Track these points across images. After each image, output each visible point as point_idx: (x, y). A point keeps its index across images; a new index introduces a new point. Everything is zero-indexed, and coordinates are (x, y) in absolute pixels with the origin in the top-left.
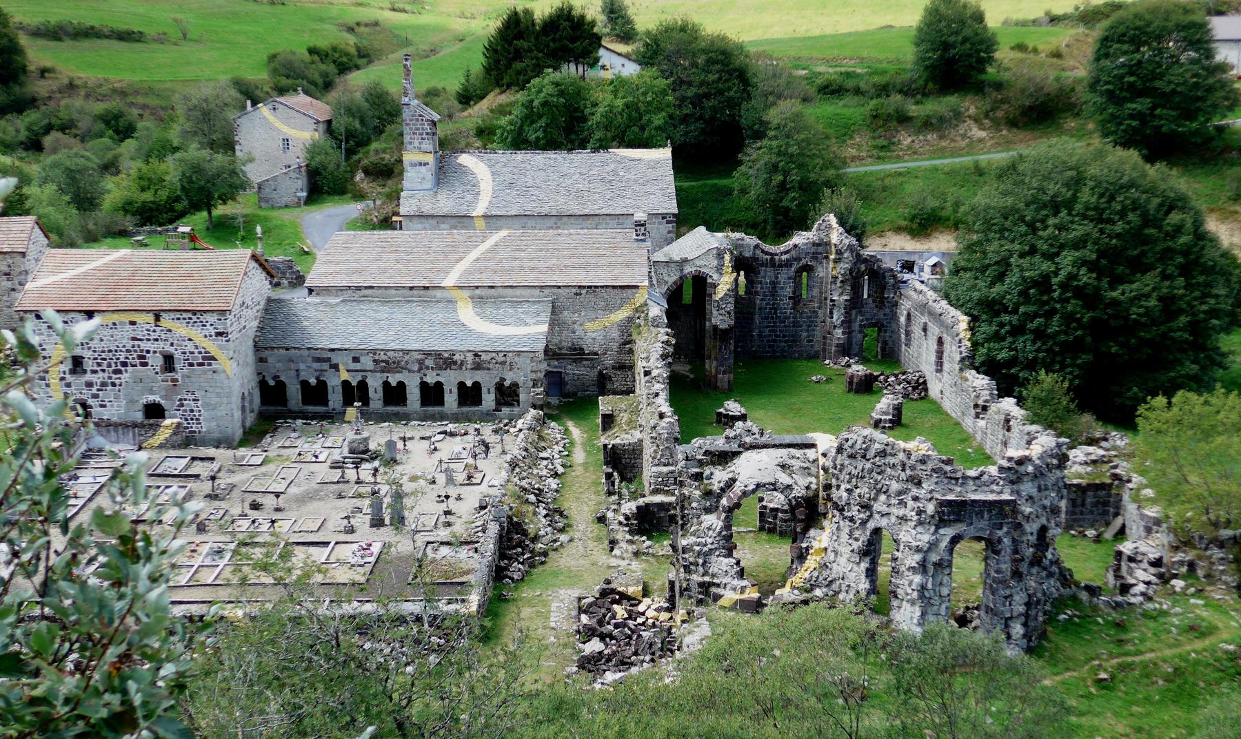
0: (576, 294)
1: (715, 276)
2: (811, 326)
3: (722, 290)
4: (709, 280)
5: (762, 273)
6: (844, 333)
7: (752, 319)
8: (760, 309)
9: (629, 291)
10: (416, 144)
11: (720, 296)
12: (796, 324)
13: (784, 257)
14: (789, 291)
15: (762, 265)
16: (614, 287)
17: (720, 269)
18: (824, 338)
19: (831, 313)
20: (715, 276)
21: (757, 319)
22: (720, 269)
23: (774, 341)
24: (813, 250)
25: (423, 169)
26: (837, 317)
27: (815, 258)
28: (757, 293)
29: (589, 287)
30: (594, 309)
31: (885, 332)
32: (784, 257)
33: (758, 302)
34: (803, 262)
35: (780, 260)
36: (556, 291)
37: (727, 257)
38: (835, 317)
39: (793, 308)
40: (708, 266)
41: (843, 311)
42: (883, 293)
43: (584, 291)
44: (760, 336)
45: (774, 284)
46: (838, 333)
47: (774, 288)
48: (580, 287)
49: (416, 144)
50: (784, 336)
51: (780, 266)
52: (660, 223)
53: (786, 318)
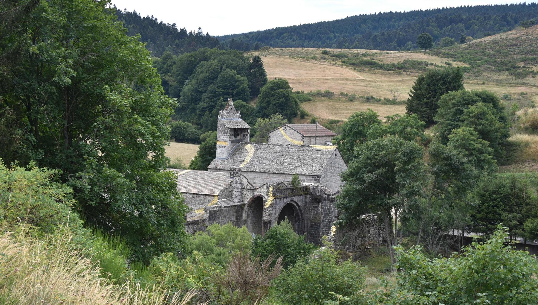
0: (193, 197)
1: (266, 197)
3: (267, 205)
4: (264, 199)
7: (319, 226)
9: (211, 197)
10: (222, 138)
11: (267, 206)
13: (333, 197)
15: (324, 200)
16: (206, 195)
20: (266, 197)
21: (322, 226)
22: (267, 193)
25: (224, 149)
29: (197, 194)
30: (199, 204)
32: (333, 197)
33: (322, 218)
35: (332, 198)
36: (186, 195)
37: (271, 189)
40: (262, 191)
43: (195, 196)
47: (329, 211)
48: (194, 194)
49: (222, 138)
51: (332, 201)
52: (312, 180)
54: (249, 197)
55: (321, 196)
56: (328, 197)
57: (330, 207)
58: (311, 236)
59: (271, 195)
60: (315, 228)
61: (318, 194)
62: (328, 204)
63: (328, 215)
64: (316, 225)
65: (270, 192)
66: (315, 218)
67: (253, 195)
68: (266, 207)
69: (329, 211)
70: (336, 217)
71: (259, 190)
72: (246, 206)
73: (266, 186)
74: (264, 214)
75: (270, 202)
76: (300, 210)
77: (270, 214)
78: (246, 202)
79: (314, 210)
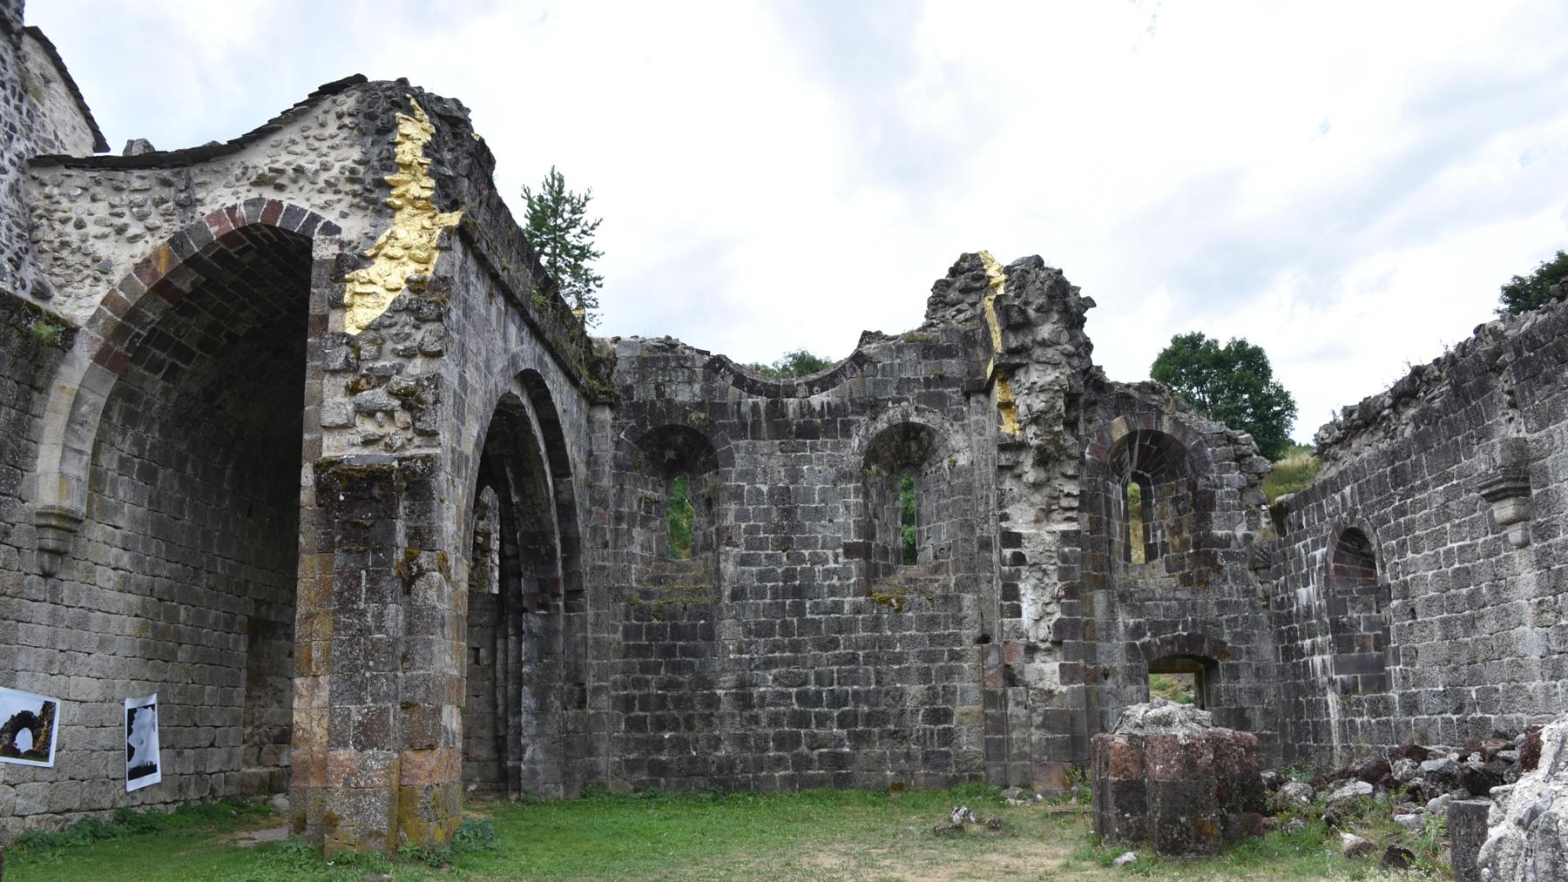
2: (939, 659)
4: (324, 250)
5: (740, 461)
6: (1067, 674)
7: (710, 634)
8: (737, 595)
12: (880, 650)
13: (817, 400)
14: (843, 522)
15: (741, 430)
17: (374, 195)
18: (991, 698)
19: (1011, 592)
20: (354, 228)
21: (729, 631)
23: (800, 720)
24: (924, 370)
26: (1035, 609)
27: (938, 402)
28: (725, 536)
31: (1234, 673)
32: (817, 400)
33: (729, 568)
34: (893, 414)
38: (1029, 610)
39: (865, 589)
41: (1055, 584)
42: (1203, 519)
44: (744, 700)
45: (785, 500)
46: (1047, 671)
47: (788, 513)
50: (837, 700)
53: (841, 626)
54: (124, 257)
55: (719, 409)
56: (776, 410)
57: (795, 476)
58: (635, 724)
59: (422, 187)
60: (668, 652)
61: (684, 394)
62: (776, 462)
63: (785, 544)
64: (678, 632)
65: (408, 152)
66: (657, 580)
67: (169, 229)
68: (357, 318)
69: (788, 513)
70: (850, 551)
71: (260, 160)
72: (83, 354)
73: (348, 102)
74: (330, 399)
75: (411, 270)
76: (567, 511)
77: (410, 400)
78: (81, 304)
79: (645, 523)
